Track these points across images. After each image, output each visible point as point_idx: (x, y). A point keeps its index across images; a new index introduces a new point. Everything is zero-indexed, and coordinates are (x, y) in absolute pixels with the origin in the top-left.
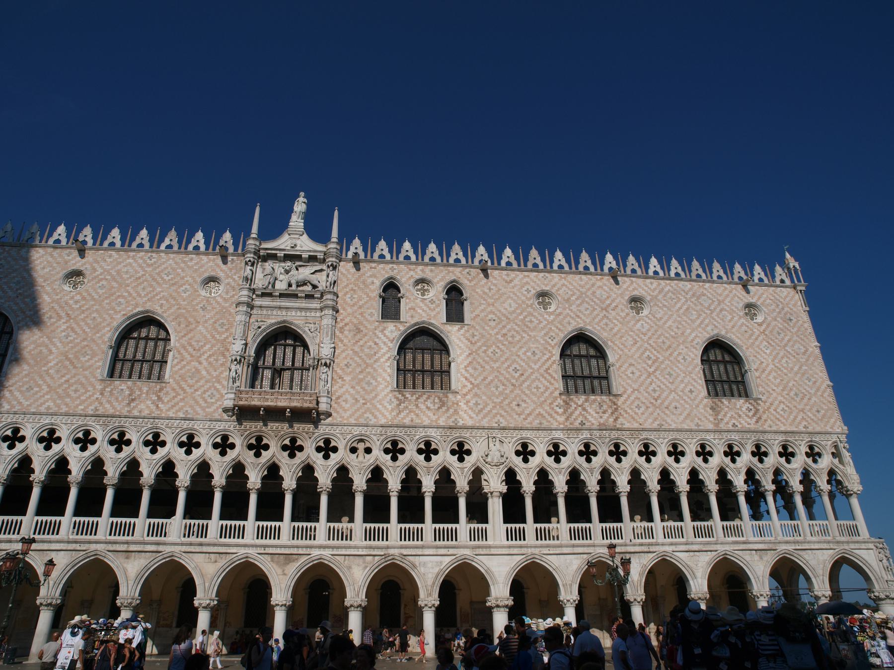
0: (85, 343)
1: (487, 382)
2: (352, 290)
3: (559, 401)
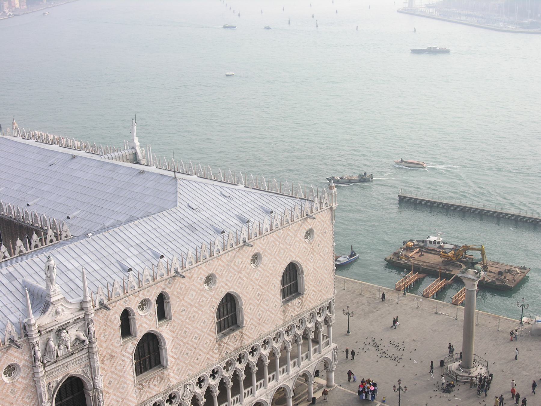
1: (182, 354)
2: (104, 330)
3: (217, 346)
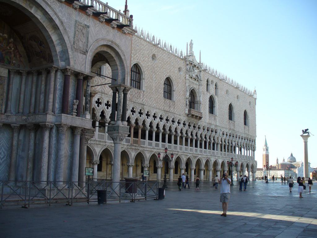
0: (159, 84)
